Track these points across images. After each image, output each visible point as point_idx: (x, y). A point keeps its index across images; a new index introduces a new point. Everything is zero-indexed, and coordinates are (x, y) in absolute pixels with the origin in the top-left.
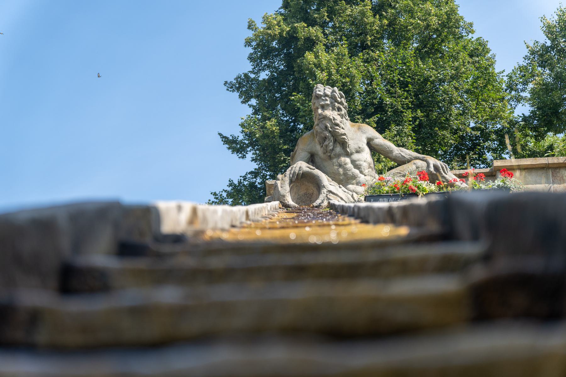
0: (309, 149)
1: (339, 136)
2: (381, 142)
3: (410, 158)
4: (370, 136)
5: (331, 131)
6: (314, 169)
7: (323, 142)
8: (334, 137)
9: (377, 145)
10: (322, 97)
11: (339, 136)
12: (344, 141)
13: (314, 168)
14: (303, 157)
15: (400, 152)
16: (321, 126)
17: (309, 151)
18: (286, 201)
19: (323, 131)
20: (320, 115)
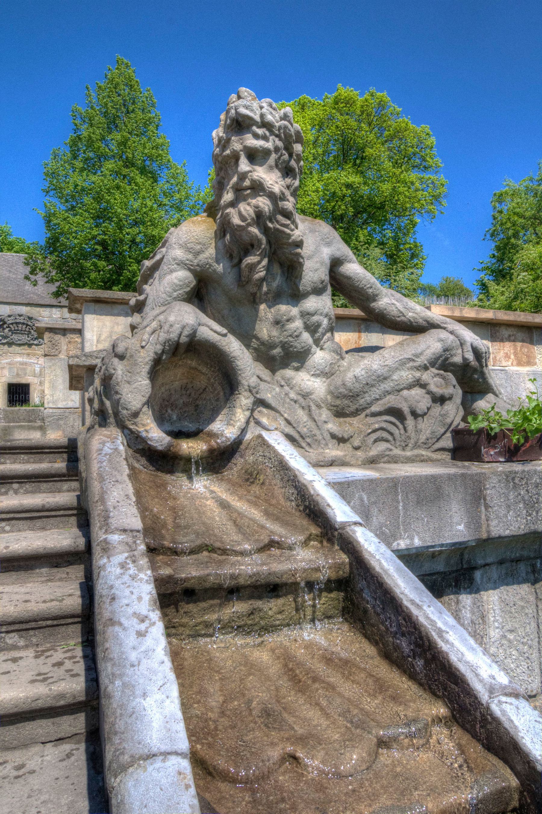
0: (198, 265)
1: (285, 246)
2: (358, 271)
3: (413, 317)
4: (338, 254)
5: (270, 228)
6: (225, 335)
7: (242, 253)
8: (273, 246)
9: (349, 278)
10: (252, 125)
11: (285, 246)
12: (295, 262)
13: (225, 331)
14: (181, 283)
15: (396, 303)
16: (242, 209)
17: (198, 269)
18: (141, 429)
19: (249, 225)
20: (243, 176)
